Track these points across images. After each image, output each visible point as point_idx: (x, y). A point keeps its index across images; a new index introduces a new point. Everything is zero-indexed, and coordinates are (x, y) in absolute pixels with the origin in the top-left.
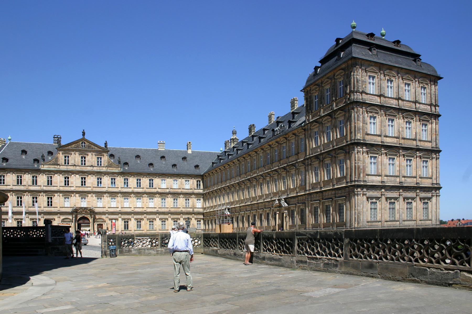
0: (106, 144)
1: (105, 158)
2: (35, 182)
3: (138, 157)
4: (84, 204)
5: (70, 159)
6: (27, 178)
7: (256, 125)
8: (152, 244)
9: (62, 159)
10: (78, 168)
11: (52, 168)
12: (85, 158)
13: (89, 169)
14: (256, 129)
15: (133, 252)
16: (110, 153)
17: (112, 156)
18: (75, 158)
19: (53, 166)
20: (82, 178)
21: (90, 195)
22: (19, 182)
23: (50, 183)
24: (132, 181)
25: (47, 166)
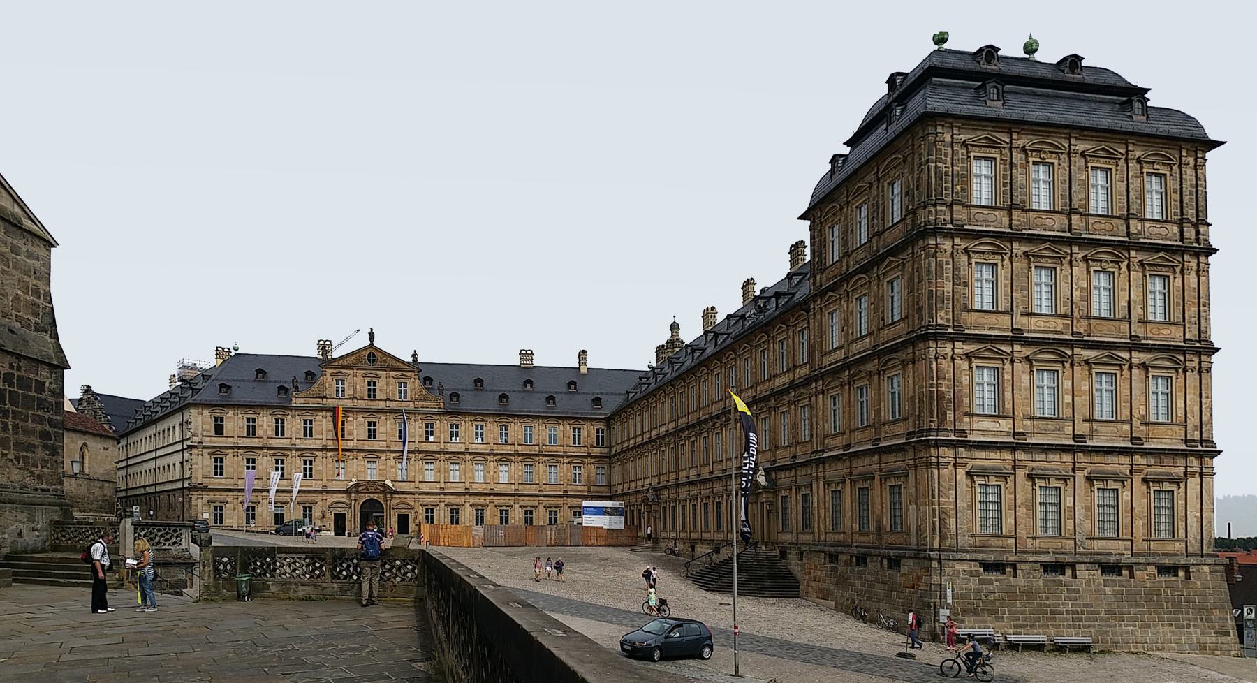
0: (415, 355)
1: (414, 385)
2: (280, 432)
3: (478, 381)
4: (371, 474)
5: (346, 386)
6: (265, 422)
7: (717, 309)
8: (313, 571)
9: (331, 386)
10: (361, 404)
11: (312, 403)
12: (375, 384)
13: (382, 405)
14: (720, 317)
15: (273, 589)
16: (422, 375)
17: (427, 380)
18: (357, 383)
19: (314, 400)
20: (369, 424)
21: (383, 456)
22: (251, 431)
23: (308, 433)
24: (467, 428)
25: (302, 400)
